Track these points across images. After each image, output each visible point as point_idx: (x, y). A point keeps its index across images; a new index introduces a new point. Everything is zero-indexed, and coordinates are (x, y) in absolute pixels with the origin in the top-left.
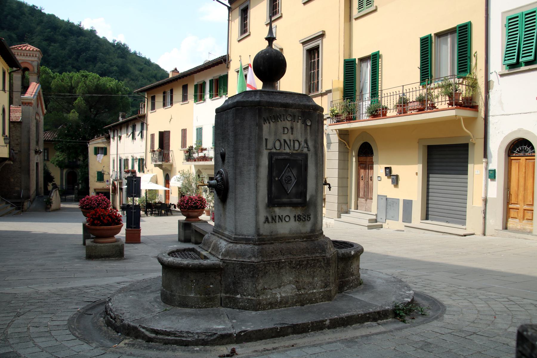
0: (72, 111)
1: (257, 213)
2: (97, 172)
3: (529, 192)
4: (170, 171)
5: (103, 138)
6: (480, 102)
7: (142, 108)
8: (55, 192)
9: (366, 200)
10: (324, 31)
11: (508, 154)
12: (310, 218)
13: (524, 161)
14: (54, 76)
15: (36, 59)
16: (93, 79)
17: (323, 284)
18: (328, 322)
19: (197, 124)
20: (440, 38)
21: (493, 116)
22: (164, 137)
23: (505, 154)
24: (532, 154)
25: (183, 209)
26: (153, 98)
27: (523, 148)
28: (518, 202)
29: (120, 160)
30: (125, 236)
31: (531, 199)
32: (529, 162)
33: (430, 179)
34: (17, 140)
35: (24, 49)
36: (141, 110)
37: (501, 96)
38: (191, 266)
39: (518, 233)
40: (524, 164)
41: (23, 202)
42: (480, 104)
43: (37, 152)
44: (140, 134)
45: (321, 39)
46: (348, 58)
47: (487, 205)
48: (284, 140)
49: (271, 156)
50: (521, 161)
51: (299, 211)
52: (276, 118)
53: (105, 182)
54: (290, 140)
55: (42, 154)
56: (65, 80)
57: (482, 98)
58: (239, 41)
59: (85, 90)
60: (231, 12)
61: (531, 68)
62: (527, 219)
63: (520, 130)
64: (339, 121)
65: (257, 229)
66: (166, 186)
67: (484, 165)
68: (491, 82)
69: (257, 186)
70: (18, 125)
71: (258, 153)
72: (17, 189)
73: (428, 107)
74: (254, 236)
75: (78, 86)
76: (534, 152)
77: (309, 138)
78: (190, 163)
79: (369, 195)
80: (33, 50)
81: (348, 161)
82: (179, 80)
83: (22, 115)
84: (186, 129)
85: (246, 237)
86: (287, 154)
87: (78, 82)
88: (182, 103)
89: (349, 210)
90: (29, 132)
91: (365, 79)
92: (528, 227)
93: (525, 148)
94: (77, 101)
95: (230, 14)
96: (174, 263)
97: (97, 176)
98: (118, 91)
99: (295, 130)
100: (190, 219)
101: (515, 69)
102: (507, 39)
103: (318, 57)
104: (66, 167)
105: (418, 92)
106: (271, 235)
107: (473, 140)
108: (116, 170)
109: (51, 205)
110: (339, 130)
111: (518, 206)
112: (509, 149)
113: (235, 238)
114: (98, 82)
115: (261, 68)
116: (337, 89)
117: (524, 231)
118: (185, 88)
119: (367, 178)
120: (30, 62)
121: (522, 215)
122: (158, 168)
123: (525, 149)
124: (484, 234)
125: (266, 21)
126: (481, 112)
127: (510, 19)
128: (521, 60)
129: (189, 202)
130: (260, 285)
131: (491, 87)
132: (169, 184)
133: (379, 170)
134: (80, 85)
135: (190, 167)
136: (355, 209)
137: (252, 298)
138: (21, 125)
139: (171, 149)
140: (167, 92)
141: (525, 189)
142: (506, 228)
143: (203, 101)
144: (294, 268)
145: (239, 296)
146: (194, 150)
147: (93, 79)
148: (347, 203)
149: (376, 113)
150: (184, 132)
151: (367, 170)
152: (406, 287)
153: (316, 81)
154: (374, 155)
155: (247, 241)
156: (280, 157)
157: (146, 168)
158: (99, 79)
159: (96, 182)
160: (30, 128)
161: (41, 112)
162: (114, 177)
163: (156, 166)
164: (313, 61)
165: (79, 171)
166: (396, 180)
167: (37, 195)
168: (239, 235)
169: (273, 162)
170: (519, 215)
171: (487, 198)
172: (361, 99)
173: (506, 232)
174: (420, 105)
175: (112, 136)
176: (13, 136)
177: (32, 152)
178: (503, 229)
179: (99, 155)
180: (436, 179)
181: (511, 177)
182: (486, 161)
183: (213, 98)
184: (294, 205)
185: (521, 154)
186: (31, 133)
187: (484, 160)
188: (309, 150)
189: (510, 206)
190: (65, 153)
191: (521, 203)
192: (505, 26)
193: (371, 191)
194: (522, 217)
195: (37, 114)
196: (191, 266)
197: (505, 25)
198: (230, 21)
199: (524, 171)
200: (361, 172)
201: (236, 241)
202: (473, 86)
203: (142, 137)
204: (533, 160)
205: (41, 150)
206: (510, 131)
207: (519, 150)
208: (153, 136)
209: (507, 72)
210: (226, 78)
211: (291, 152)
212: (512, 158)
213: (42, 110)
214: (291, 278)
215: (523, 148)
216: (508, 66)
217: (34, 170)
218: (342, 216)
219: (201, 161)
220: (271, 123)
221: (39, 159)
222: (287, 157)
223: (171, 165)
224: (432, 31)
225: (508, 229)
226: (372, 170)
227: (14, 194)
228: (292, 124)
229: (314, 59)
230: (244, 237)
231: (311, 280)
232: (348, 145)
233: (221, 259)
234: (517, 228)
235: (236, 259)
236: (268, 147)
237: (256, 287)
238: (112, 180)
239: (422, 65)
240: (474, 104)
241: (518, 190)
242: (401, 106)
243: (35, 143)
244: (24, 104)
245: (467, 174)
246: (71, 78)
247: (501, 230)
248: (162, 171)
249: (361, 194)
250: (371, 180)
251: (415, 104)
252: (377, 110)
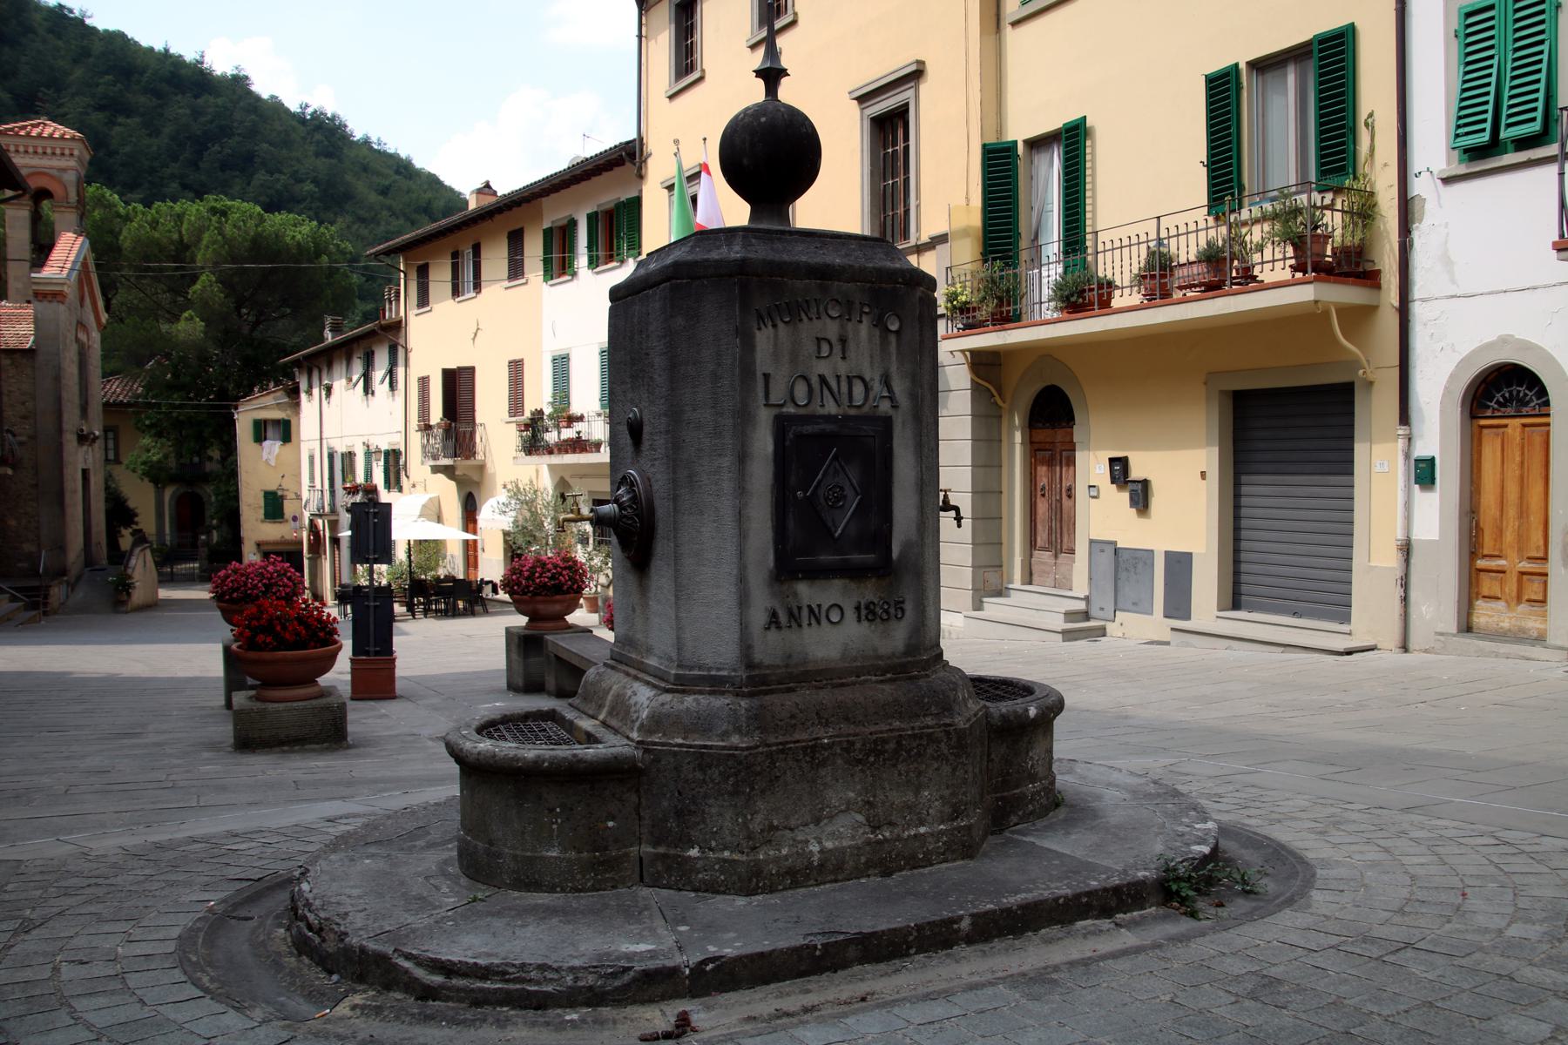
0: (186, 314)
1: (743, 601)
2: (262, 494)
3: (1535, 519)
4: (478, 484)
5: (279, 394)
6: (1387, 261)
7: (391, 302)
9: (1056, 557)
10: (921, 63)
11: (1471, 413)
12: (903, 611)
13: (1519, 430)
14: (127, 215)
15: (72, 163)
16: (243, 221)
17: (948, 810)
18: (965, 924)
19: (552, 346)
20: (1263, 74)
21: (1423, 300)
22: (458, 385)
23: (1462, 412)
24: (1542, 408)
25: (518, 594)
26: (423, 272)
27: (1515, 393)
28: (1501, 551)
29: (331, 456)
30: (349, 677)
31: (1541, 543)
32: (1533, 432)
33: (1244, 489)
34: (23, 403)
35: (35, 133)
36: (387, 306)
37: (1446, 242)
38: (546, 764)
39: (1506, 642)
40: (1518, 438)
42: (1387, 267)
43: (83, 438)
44: (388, 377)
45: (913, 84)
46: (994, 141)
47: (1413, 561)
48: (820, 376)
49: (782, 425)
50: (1509, 430)
51: (869, 592)
52: (794, 311)
53: (287, 521)
54: (838, 377)
55: (99, 444)
56: (163, 224)
57: (1392, 249)
58: (671, 97)
59: (224, 252)
60: (646, 12)
61: (1533, 158)
62: (1529, 601)
63: (1504, 340)
64: (972, 326)
65: (746, 648)
66: (466, 530)
67: (1401, 443)
68: (1416, 202)
69: (740, 517)
70: (25, 361)
71: (744, 418)
72: (28, 547)
73: (1235, 278)
74: (735, 670)
75: (199, 240)
76: (1547, 403)
77: (894, 369)
78: (534, 459)
79: (1065, 539)
80: (62, 138)
81: (1001, 441)
82: (498, 217)
83: (36, 329)
84: (522, 361)
85: (713, 673)
86: (829, 418)
87: (201, 231)
88: (507, 284)
89: (1005, 585)
90: (58, 378)
91: (1044, 203)
92: (1533, 624)
93: (1519, 392)
94: (198, 286)
95: (644, 18)
96: (494, 756)
97: (262, 504)
98: (318, 254)
99: (851, 345)
100: (540, 624)
101: (1487, 160)
102: (1461, 74)
103: (906, 138)
104: (173, 480)
105: (1202, 235)
106: (787, 666)
107: (1368, 371)
108: (318, 486)
109: (129, 594)
110: (972, 352)
111: (1502, 562)
112: (1474, 398)
113: (677, 676)
114: (260, 229)
115: (745, 161)
116: (965, 232)
117: (1522, 636)
118: (516, 241)
119: (1058, 490)
121: (1515, 590)
122: (441, 476)
123: (1521, 395)
124: (1405, 648)
125: (749, 36)
126: (1389, 289)
127: (1469, 15)
128: (1503, 135)
129: (537, 575)
130: (759, 818)
131: (1416, 215)
132: (475, 522)
133: (1092, 466)
134: (206, 237)
135: (537, 471)
136: (1023, 584)
137: (736, 857)
139: (478, 421)
140: (463, 251)
141: (1523, 512)
142: (1467, 628)
143: (570, 278)
144: (859, 761)
145: (694, 852)
146: (548, 422)
147: (243, 221)
148: (1001, 566)
149: (1081, 300)
150: (516, 368)
151: (1058, 469)
152: (1195, 809)
153: (901, 211)
154: (1077, 422)
155: (715, 684)
156: (809, 429)
157: (408, 477)
158: (262, 220)
159: (262, 521)
160: (60, 368)
161: (92, 318)
162: (313, 507)
163: (436, 470)
164: (890, 150)
165: (209, 492)
166: (1141, 496)
167: (86, 566)
168: (691, 668)
169: (787, 443)
170: (1507, 590)
171: (1412, 542)
172: (1036, 261)
173: (1468, 641)
174: (1208, 272)
175: (303, 386)
176: (10, 392)
177: (70, 440)
178: (1460, 631)
179: (266, 444)
180: (1262, 492)
181: (1479, 477)
182: (1407, 432)
183: (597, 266)
184: (854, 573)
185: (1510, 411)
186: (63, 381)
187: (1402, 431)
188: (895, 407)
189: (1481, 563)
190: (168, 440)
191: (1513, 554)
192: (1456, 36)
193: (1068, 530)
194: (1514, 594)
195: (81, 325)
196: (546, 764)
197: (1456, 31)
198: (643, 39)
199: (1518, 459)
200: (1038, 473)
201: (681, 685)
202: (1364, 213)
203: (392, 386)
204: (1543, 428)
205: (97, 433)
206: (1476, 345)
207: (1501, 400)
208: (424, 382)
209: (1463, 170)
210: (635, 204)
211: (841, 412)
212: (1483, 422)
213: (95, 315)
214: (852, 795)
215: (1515, 393)
216: (1466, 151)
217: (75, 492)
218: (985, 604)
219: (567, 452)
220: (781, 325)
221: (90, 460)
222: (829, 427)
223: (481, 468)
224: (1242, 55)
225: (1475, 630)
226: (1072, 468)
227: (20, 565)
228: (842, 327)
229: (895, 144)
230: (705, 673)
231: (910, 797)
232: (1000, 395)
233: (638, 742)
234: (1501, 628)
235: (684, 739)
236: (773, 400)
237: (745, 824)
238: (307, 515)
239: (1213, 156)
240: (1369, 267)
241: (1502, 515)
242: (1153, 277)
243: (77, 412)
244: (40, 298)
245: (1352, 474)
246: (180, 217)
247: (1454, 635)
248: (453, 484)
249: (1042, 538)
250: (1069, 497)
251: (1195, 269)
252: (1084, 291)
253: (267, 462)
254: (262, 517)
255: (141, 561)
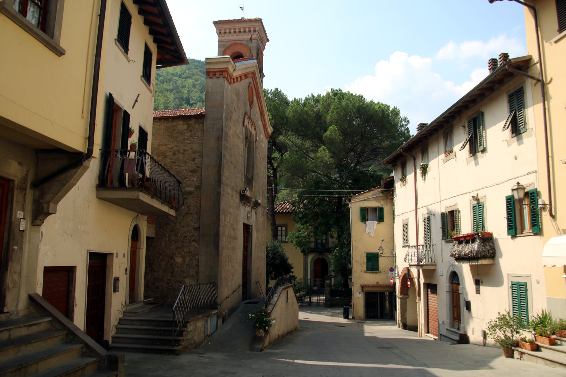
0: (321, 148)
2: (365, 255)
8: (285, 292)
29: (428, 220)
34: (194, 160)
41: (185, 323)
59: (342, 114)
90: (219, 139)
94: (328, 133)
97: (365, 261)
104: (312, 251)
109: (267, 332)
120: (245, 42)
138: (203, 123)
157: (553, 217)
159: (365, 272)
165: (331, 258)
176: (184, 150)
179: (368, 223)
186: (224, 142)
190: (310, 225)
253: (369, 234)
254: (366, 270)
255: (283, 297)
